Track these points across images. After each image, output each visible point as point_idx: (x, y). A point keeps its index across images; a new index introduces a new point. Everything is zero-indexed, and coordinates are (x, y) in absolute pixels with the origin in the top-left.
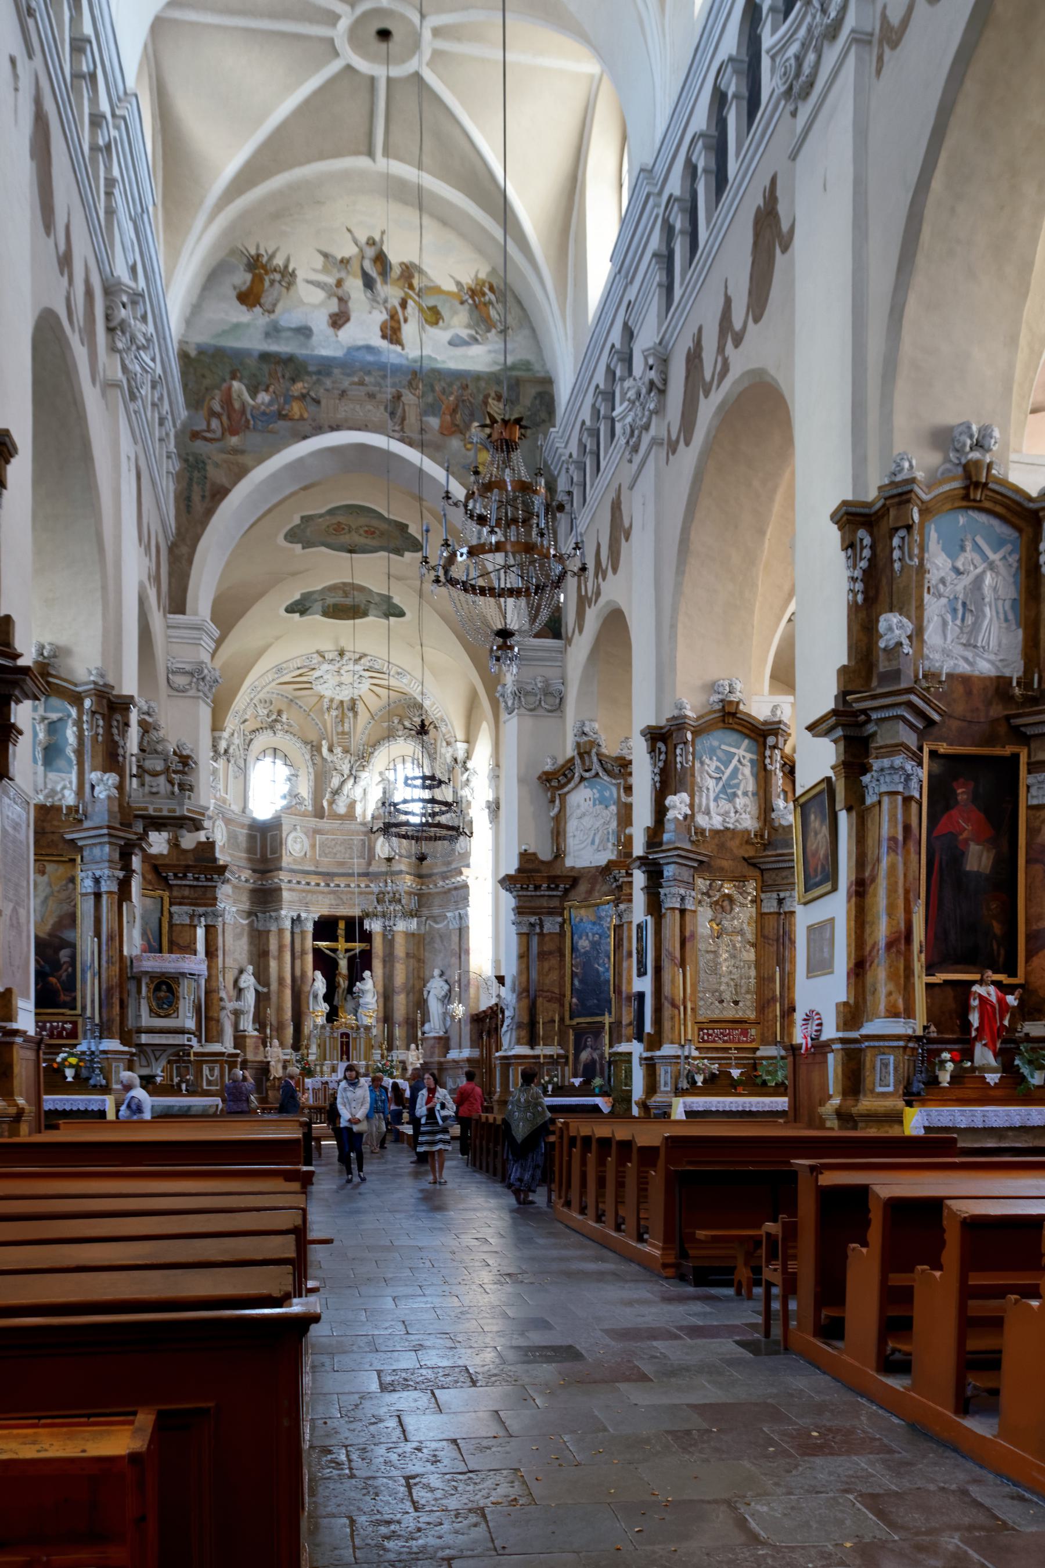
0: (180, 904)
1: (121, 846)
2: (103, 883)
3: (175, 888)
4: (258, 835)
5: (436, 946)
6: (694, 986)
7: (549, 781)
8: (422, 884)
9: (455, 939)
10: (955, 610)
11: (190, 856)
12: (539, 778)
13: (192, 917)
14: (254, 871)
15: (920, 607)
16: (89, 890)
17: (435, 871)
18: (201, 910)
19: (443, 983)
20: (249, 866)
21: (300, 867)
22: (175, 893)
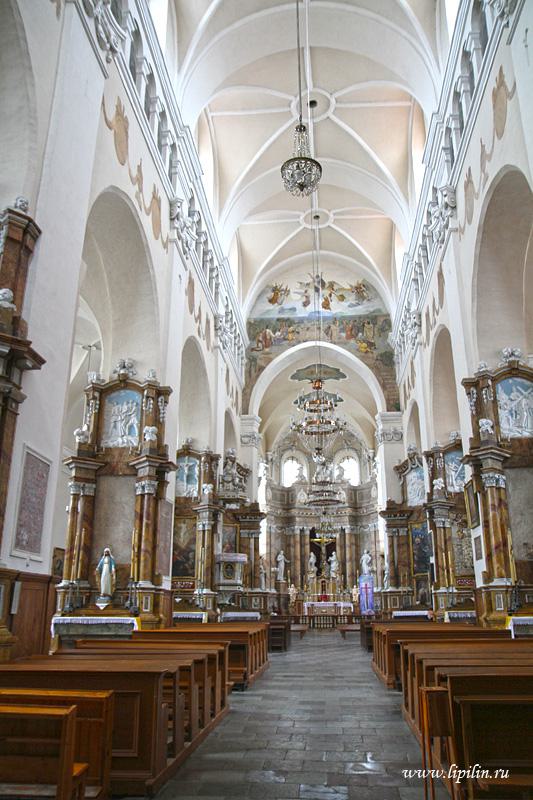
6: (453, 560)
9: (373, 535)
10: (512, 415)
14: (284, 509)
15: (496, 415)
18: (252, 531)
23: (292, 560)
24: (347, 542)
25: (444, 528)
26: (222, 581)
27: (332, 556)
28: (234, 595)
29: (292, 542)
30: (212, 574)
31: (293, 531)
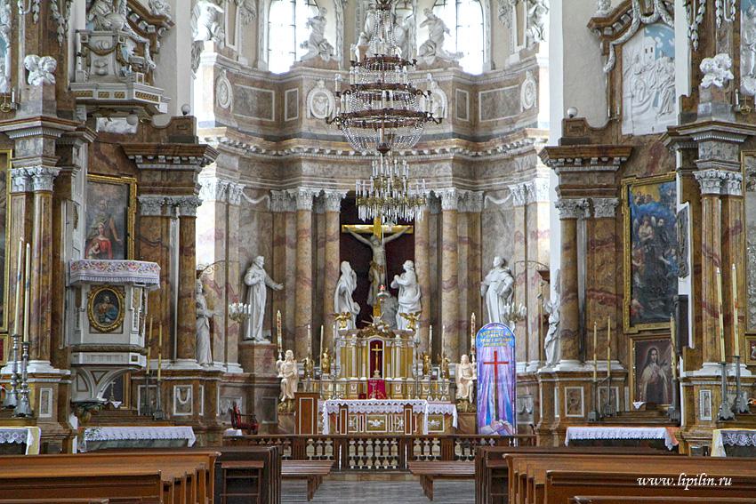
0: (151, 192)
1: (57, 139)
2: (36, 181)
3: (145, 173)
4: (273, 92)
5: (497, 227)
6: (743, 289)
7: (600, 29)
8: (478, 150)
9: (520, 218)
11: (163, 134)
12: (589, 25)
13: (164, 207)
14: (267, 138)
16: (20, 190)
17: (495, 132)
18: (175, 198)
19: (505, 275)
20: (261, 132)
21: (325, 133)
22: (145, 179)
23: (290, 282)
24: (447, 236)
25: (724, 198)
26: (85, 337)
27: (401, 271)
28: (119, 380)
29: (290, 232)
30: (55, 318)
31: (294, 199)
